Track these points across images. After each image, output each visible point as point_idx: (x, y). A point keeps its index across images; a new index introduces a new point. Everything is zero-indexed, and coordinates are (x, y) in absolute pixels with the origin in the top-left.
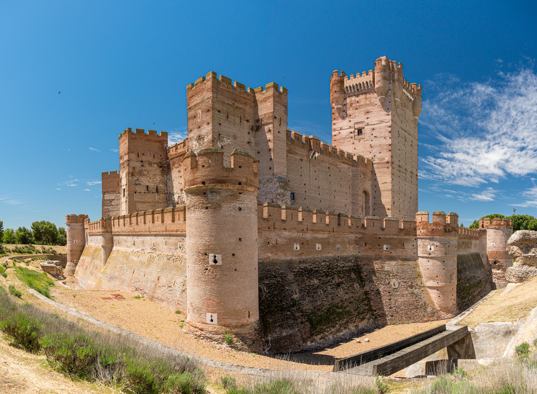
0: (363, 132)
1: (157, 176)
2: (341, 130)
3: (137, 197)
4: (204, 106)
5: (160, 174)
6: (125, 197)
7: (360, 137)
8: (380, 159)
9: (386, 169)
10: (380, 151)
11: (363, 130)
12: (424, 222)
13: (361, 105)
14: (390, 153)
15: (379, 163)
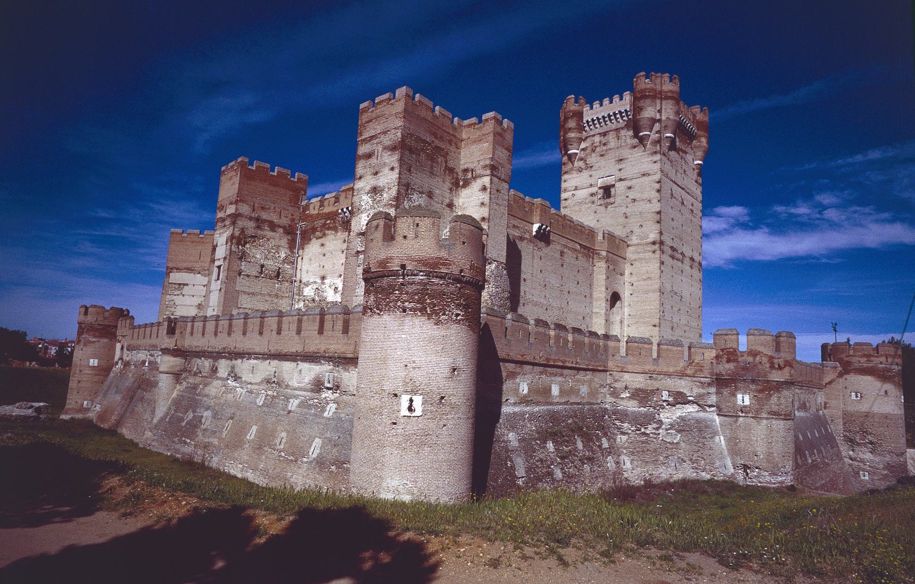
0: (612, 193)
1: (281, 249)
2: (575, 190)
3: (241, 284)
4: (387, 140)
5: (287, 246)
6: (219, 282)
7: (608, 200)
8: (642, 238)
9: (650, 253)
10: (640, 224)
11: (612, 190)
12: (730, 348)
13: (610, 149)
14: (658, 226)
15: (638, 245)
